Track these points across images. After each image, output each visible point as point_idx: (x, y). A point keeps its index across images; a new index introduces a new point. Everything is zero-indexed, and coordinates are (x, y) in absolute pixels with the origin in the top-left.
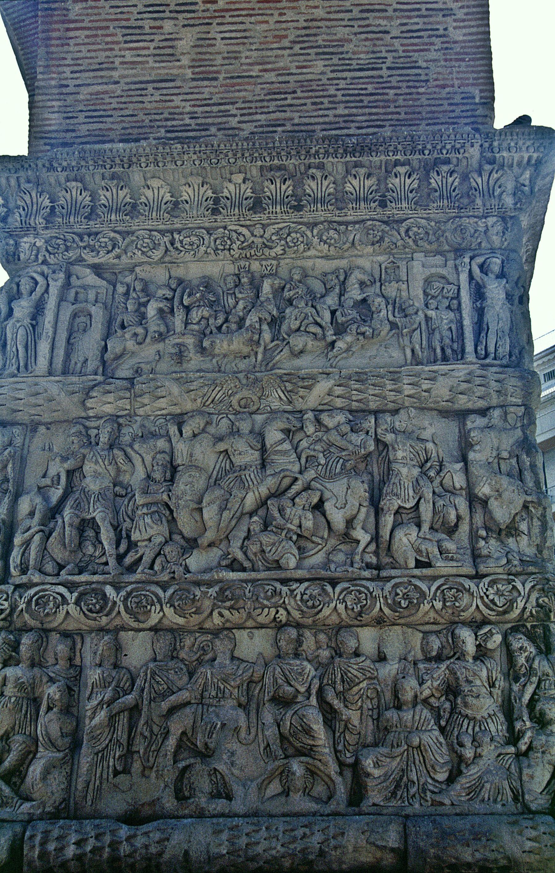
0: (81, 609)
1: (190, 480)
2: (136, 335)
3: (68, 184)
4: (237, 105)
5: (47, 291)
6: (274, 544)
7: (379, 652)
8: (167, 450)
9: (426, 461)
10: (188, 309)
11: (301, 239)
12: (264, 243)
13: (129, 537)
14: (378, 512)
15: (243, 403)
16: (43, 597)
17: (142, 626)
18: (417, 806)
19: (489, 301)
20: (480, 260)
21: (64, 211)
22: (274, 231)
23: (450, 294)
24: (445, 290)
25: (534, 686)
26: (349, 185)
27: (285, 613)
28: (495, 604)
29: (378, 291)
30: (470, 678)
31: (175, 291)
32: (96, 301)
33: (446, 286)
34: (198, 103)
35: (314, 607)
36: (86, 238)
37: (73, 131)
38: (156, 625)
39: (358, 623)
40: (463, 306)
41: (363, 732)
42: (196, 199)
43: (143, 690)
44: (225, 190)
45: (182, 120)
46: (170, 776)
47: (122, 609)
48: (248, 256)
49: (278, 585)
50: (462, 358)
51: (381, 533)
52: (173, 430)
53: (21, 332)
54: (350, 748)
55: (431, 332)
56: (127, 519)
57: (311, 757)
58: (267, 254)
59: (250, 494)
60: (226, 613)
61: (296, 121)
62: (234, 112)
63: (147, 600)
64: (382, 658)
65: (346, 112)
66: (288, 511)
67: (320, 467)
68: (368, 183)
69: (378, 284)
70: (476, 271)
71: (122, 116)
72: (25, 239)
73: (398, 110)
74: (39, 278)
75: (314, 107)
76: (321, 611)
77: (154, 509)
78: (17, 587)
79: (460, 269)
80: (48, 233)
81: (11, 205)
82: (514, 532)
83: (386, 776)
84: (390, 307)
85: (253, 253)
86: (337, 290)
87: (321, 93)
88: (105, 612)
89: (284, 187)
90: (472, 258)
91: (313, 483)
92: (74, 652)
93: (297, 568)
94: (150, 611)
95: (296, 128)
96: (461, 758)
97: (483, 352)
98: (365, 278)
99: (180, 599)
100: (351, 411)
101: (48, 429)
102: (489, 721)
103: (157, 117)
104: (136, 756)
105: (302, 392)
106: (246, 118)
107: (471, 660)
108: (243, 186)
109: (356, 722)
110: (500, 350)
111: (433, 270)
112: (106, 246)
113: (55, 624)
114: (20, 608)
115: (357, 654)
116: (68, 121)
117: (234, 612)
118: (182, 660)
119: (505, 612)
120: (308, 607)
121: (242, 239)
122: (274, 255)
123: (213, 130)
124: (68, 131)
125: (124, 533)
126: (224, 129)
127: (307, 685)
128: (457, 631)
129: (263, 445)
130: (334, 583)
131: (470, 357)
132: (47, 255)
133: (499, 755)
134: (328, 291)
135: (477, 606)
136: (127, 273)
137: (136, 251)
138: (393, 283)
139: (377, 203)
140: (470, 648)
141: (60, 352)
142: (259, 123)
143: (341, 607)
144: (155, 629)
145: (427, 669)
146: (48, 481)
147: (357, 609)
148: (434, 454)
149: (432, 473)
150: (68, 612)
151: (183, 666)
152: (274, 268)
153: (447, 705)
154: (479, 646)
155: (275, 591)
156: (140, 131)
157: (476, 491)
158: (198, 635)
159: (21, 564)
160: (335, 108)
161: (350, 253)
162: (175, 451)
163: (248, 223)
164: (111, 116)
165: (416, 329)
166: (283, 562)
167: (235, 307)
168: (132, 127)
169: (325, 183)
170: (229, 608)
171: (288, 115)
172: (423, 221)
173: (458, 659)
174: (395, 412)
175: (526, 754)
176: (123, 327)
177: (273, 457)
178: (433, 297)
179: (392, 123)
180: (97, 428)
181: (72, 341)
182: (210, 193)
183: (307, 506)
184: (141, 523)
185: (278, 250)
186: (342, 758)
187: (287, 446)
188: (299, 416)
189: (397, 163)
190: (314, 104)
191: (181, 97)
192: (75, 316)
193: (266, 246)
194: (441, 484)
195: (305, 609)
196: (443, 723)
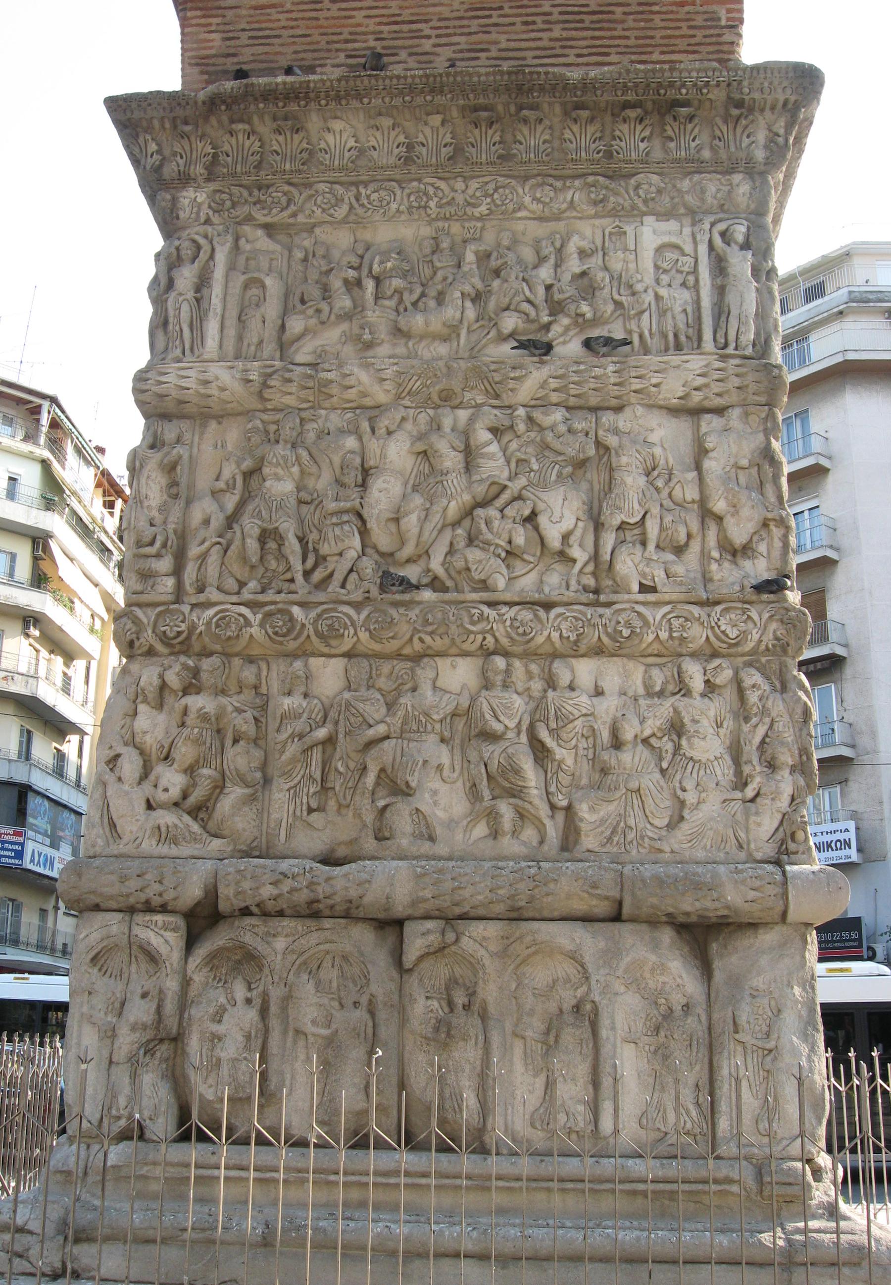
0: (266, 632)
1: (385, 485)
2: (318, 311)
3: (234, 126)
4: (431, 24)
5: (212, 257)
6: (480, 562)
7: (596, 686)
8: (357, 450)
9: (654, 469)
10: (378, 280)
11: (510, 196)
12: (466, 200)
13: (315, 550)
14: (598, 526)
15: (444, 394)
16: (224, 618)
17: (333, 651)
19: (731, 278)
20: (722, 226)
21: (229, 159)
22: (477, 186)
23: (686, 269)
24: (680, 263)
25: (766, 727)
26: (567, 131)
28: (727, 636)
29: (600, 262)
30: (697, 718)
31: (362, 257)
32: (270, 270)
33: (681, 258)
34: (385, 20)
35: (524, 634)
36: (256, 193)
37: (234, 55)
38: (349, 651)
39: (573, 653)
40: (702, 283)
41: (577, 774)
42: (386, 145)
43: (337, 723)
44: (421, 135)
45: (365, 41)
46: (369, 818)
47: (312, 633)
48: (448, 215)
49: (486, 610)
50: (699, 346)
51: (601, 552)
52: (365, 426)
53: (185, 308)
54: (564, 790)
55: (662, 313)
56: (315, 531)
57: (521, 798)
58: (470, 213)
59: (453, 504)
60: (428, 639)
61: (503, 45)
62: (427, 32)
63: (339, 623)
64: (599, 692)
65: (565, 34)
66: (496, 524)
67: (532, 474)
68: (591, 129)
69: (600, 253)
70: (718, 241)
71: (293, 36)
72: (185, 194)
73: (627, 33)
74: (202, 241)
75: (524, 28)
76: (532, 639)
77: (345, 518)
78: (194, 606)
79: (698, 237)
80: (212, 186)
81: (167, 152)
82: (750, 554)
83: (602, 821)
84: (615, 284)
85: (453, 213)
86: (552, 261)
87: (533, 10)
88: (293, 636)
89: (490, 132)
90: (712, 225)
91: (524, 492)
92: (260, 680)
93: (506, 589)
94: (343, 635)
95: (504, 54)
96: (682, 803)
97: (723, 341)
99: (376, 622)
100: (568, 408)
101: (220, 423)
102: (715, 763)
103: (335, 38)
104: (330, 793)
105: (512, 384)
106: (443, 40)
107: (698, 698)
108: (442, 131)
109: (570, 761)
110: (742, 338)
111: (666, 239)
112: (279, 202)
113: (237, 649)
114: (198, 631)
115: (572, 688)
116: (228, 43)
117: (437, 638)
118: (380, 690)
119: (736, 645)
120: (518, 634)
121: (441, 195)
122: (478, 215)
123: (403, 55)
124: (228, 55)
125: (310, 545)
126: (416, 54)
127: (517, 720)
128: (684, 666)
129: (467, 446)
130: (548, 606)
131: (708, 344)
132: (211, 213)
133: (724, 801)
134: (541, 260)
135: (707, 638)
136: (305, 235)
137: (315, 209)
138: (620, 254)
139: (601, 154)
140: (697, 684)
141: (231, 333)
142: (459, 47)
143: (555, 635)
144: (349, 655)
145: (649, 706)
146: (221, 485)
147: (573, 637)
148: (662, 462)
149: (660, 483)
150: (251, 636)
151: (379, 696)
152: (478, 231)
153: (669, 746)
154: (707, 682)
155: (482, 615)
156: (316, 55)
157: (710, 505)
158: (395, 662)
159: (198, 581)
160: (550, 30)
161: (568, 214)
162: (367, 451)
163: (447, 175)
164: (279, 37)
165: (644, 311)
166: (490, 582)
167: (432, 278)
168: (305, 51)
169: (540, 128)
170: (431, 633)
171: (493, 36)
172: (655, 177)
173: (684, 695)
174: (619, 409)
175: (753, 800)
176: (303, 302)
178: (665, 271)
179: (619, 50)
180: (276, 422)
181: (243, 318)
182: (402, 138)
184: (330, 535)
185: (483, 209)
186: (555, 800)
187: (494, 448)
188: (509, 412)
189: (626, 105)
190: (526, 23)
191: (364, 13)
192: (246, 286)
193: (469, 204)
194: (670, 495)
196: (665, 765)
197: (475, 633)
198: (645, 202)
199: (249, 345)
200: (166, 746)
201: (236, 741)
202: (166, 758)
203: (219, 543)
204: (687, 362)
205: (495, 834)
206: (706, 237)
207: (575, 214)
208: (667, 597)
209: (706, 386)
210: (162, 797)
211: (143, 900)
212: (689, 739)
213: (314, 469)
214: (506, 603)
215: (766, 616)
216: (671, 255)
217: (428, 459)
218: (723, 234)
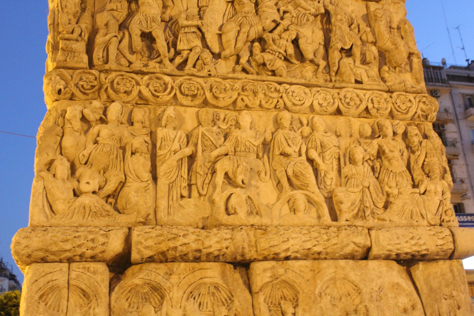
0: (150, 90)
9: (351, 25)
18: (371, 221)
27: (283, 103)
30: (392, 149)
43: (196, 145)
57: (307, 190)
66: (277, 42)
67: (293, 19)
127: (299, 148)
140: (390, 132)
148: (355, 21)
150: (140, 92)
175: (424, 194)
177: (264, 9)
183: (289, 40)
184: (184, 39)
195: (294, 101)
197: (273, 98)
200: (87, 155)
201: (133, 154)
202: (86, 163)
203: (116, 36)
205: (294, 210)
208: (368, 87)
210: (84, 187)
211: (80, 253)
212: (389, 161)
214: (287, 83)
215: (417, 100)
217: (233, 6)
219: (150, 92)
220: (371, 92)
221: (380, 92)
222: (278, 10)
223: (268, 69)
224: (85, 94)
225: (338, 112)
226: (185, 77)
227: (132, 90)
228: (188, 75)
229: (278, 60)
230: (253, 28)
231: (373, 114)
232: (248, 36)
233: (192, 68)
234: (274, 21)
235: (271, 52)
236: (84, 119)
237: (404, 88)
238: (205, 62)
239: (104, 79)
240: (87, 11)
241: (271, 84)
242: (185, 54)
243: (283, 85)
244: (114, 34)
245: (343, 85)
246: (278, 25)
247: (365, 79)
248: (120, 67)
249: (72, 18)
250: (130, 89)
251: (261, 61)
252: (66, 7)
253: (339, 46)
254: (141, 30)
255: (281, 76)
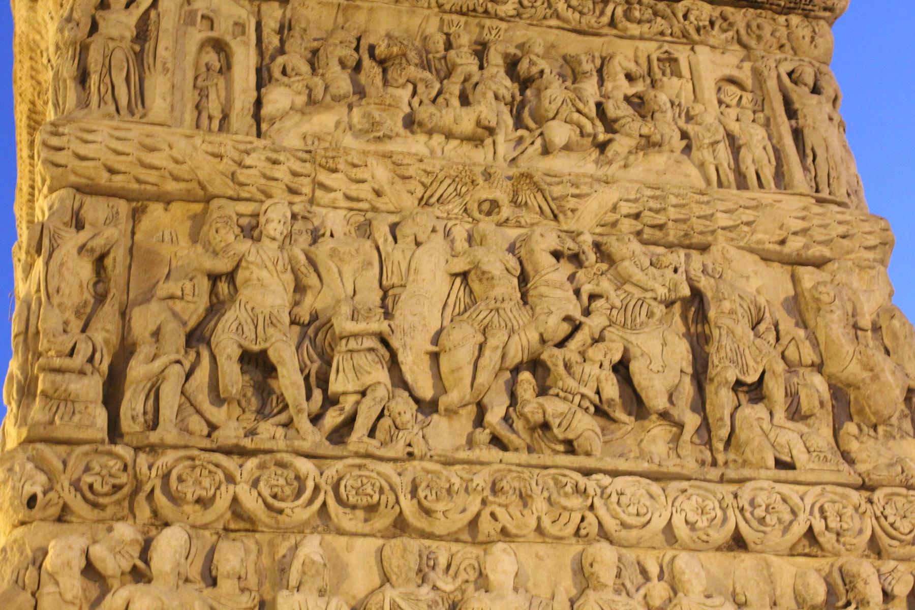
0: (259, 494)
9: (758, 323)
48: (465, 9)
53: (119, 56)
66: (577, 369)
67: (615, 312)
70: (786, 80)
98: (632, 67)
105: (572, 203)
148: (767, 314)
150: (235, 500)
177: (543, 290)
183: (607, 365)
195: (625, 517)
198: (698, 30)
199: (210, 118)
203: (178, 362)
204: (780, 201)
206: (774, 74)
207: (615, 32)
208: (810, 477)
209: (804, 232)
213: (313, 279)
214: (605, 472)
216: (732, 89)
217: (467, 284)
218: (790, 74)
219: (260, 500)
220: (818, 489)
221: (840, 490)
222: (577, 292)
223: (555, 437)
224: (95, 505)
225: (738, 543)
226: (350, 461)
227: (214, 495)
228: (357, 455)
229: (580, 415)
230: (515, 338)
231: (827, 546)
232: (503, 357)
233: (366, 439)
234: (567, 319)
235: (562, 394)
236: (90, 570)
237: (903, 477)
238: (398, 422)
239: (145, 469)
240: (109, 300)
241: (565, 476)
242: (348, 403)
243: (594, 476)
244: (174, 357)
245: (747, 472)
246: (577, 328)
247: (801, 457)
248: (187, 437)
249: (72, 318)
250: (211, 493)
251: (539, 418)
252: (58, 292)
253: (732, 375)
254: (240, 346)
255: (588, 454)
